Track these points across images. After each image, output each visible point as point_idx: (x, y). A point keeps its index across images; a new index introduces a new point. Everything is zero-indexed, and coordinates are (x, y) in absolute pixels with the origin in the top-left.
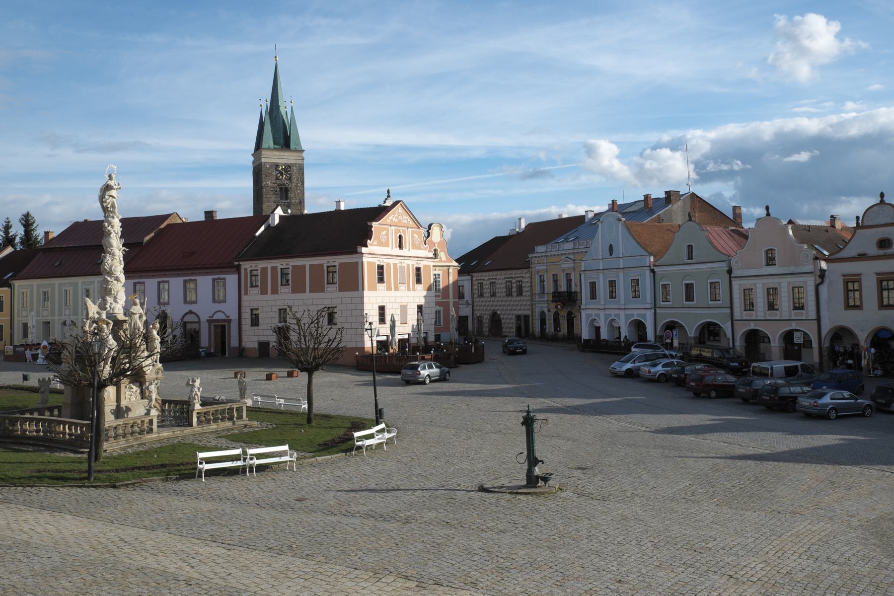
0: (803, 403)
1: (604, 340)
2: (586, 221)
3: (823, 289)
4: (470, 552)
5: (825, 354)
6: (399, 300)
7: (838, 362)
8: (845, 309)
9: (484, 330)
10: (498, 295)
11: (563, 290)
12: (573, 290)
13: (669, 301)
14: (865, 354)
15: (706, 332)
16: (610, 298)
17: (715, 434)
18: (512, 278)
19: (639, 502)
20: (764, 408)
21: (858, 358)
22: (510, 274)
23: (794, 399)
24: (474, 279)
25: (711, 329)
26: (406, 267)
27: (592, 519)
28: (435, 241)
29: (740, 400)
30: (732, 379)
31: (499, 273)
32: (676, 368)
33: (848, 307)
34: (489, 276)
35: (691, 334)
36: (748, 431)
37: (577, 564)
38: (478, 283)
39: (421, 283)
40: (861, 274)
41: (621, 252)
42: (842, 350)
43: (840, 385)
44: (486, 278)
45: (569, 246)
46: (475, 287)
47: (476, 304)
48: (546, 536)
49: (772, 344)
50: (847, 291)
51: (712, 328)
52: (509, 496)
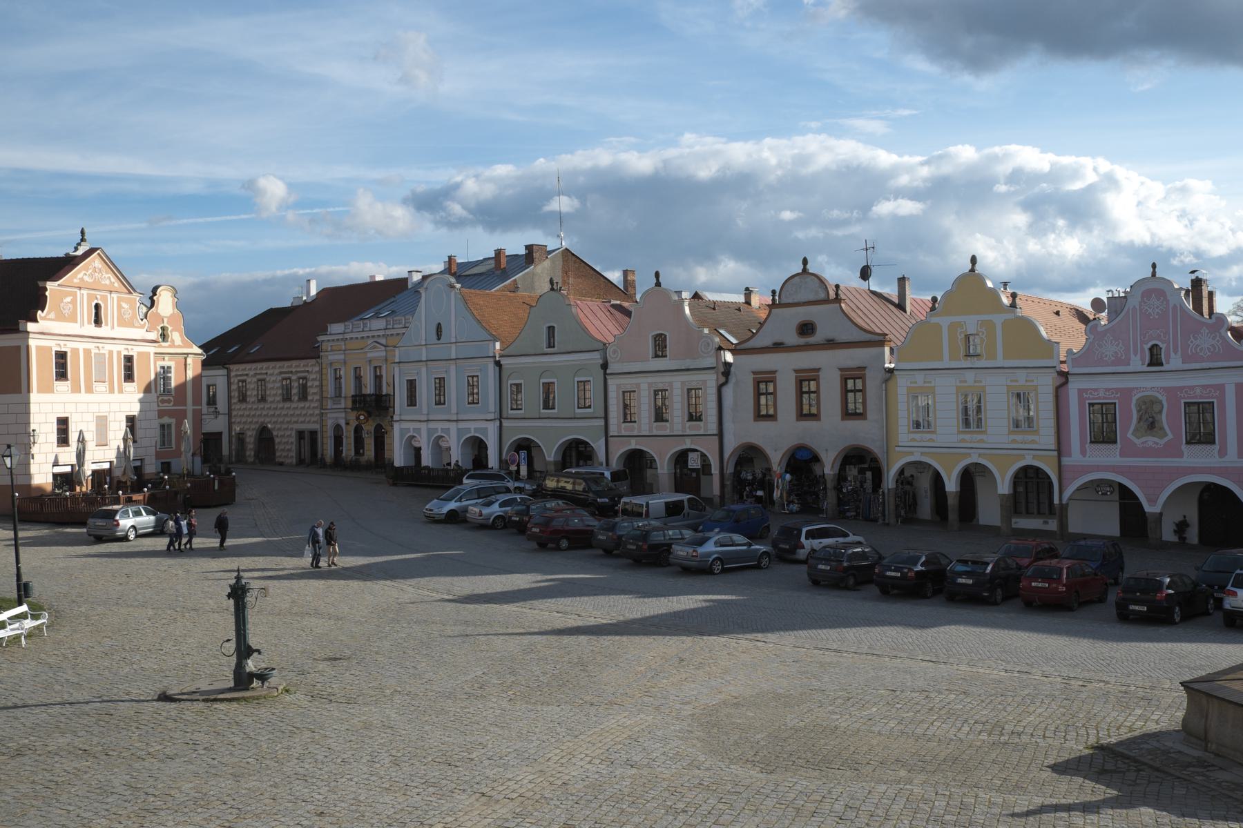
0: (679, 553)
1: (427, 468)
2: (409, 287)
3: (728, 392)
5: (728, 483)
6: (94, 408)
7: (745, 493)
8: (755, 420)
9: (248, 453)
10: (269, 399)
11: (369, 392)
12: (384, 392)
13: (521, 409)
14: (778, 482)
15: (574, 454)
16: (436, 404)
18: (291, 372)
20: (630, 561)
22: (288, 367)
24: (233, 374)
25: (581, 449)
26: (107, 356)
28: (162, 314)
29: (601, 552)
30: (593, 522)
31: (272, 364)
32: (520, 508)
33: (759, 416)
34: (255, 369)
35: (550, 456)
36: (595, 595)
38: (239, 381)
39: (133, 381)
40: (776, 371)
41: (453, 335)
42: (750, 478)
43: (736, 525)
44: (252, 373)
45: (379, 324)
46: (234, 387)
47: (234, 413)
49: (659, 471)
50: (758, 394)
52: (201, 705)
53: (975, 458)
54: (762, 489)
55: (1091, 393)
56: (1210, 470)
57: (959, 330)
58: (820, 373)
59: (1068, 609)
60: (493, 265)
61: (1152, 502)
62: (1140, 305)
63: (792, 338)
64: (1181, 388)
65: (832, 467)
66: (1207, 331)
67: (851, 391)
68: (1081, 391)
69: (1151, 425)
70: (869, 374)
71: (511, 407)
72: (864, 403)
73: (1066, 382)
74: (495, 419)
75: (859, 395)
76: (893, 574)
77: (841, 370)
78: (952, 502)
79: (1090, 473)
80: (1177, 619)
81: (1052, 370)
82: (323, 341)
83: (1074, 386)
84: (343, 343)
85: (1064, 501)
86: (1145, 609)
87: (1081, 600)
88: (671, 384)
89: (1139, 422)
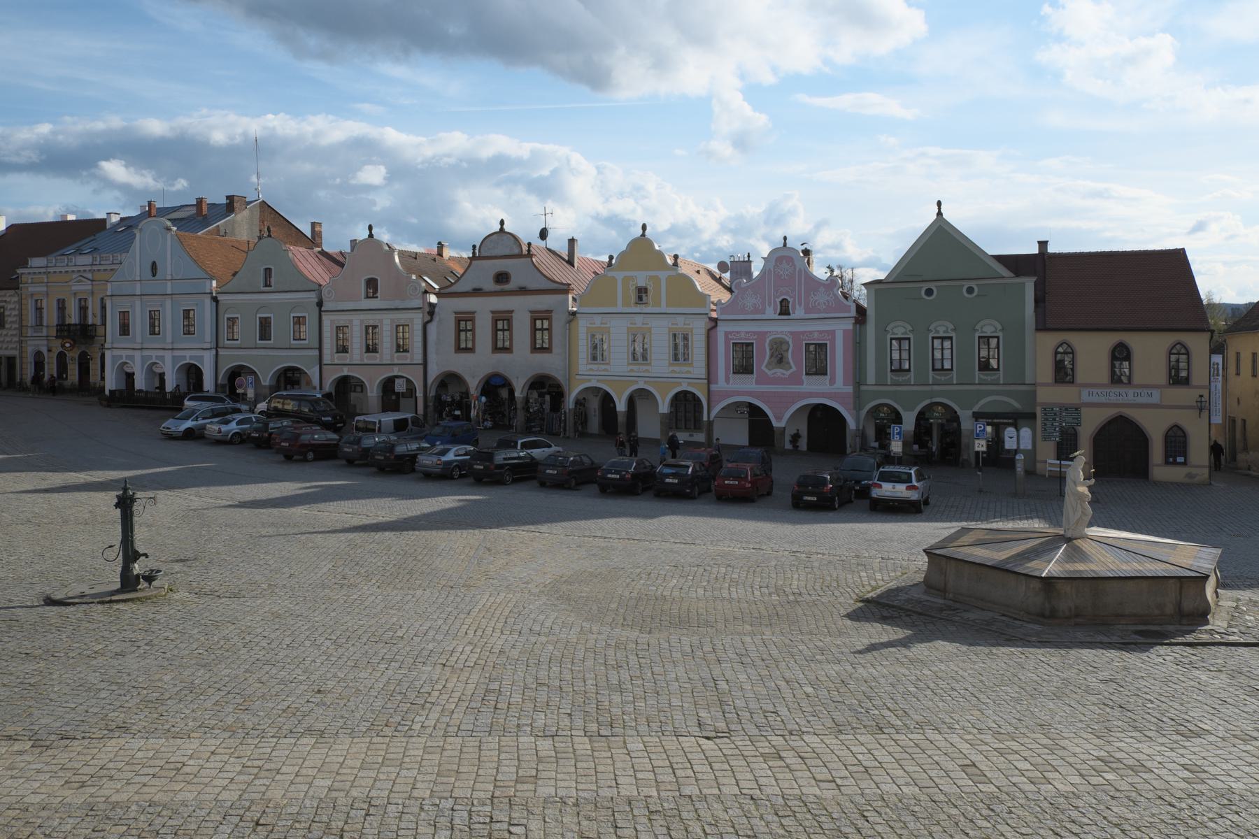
1: (140, 391)
2: (108, 227)
3: (433, 329)
4: (89, 688)
7: (444, 414)
8: (456, 352)
11: (73, 322)
15: (282, 379)
17: (331, 503)
20: (374, 469)
21: (467, 409)
23: (413, 458)
27: (236, 622)
29: (344, 462)
30: (333, 436)
33: (459, 349)
35: (265, 381)
36: (369, 498)
37: (251, 681)
42: (449, 400)
43: (456, 439)
45: (86, 260)
48: (187, 652)
49: (369, 394)
50: (459, 330)
51: (289, 374)
52: (100, 607)
53: (641, 385)
54: (460, 408)
56: (823, 395)
57: (631, 283)
59: (753, 501)
61: (779, 419)
62: (774, 268)
63: (490, 285)
64: (803, 333)
67: (539, 330)
68: (727, 334)
70: (554, 316)
72: (511, 340)
73: (716, 326)
75: (546, 333)
76: (613, 476)
77: (531, 312)
78: (621, 419)
80: (837, 506)
81: (705, 316)
82: (22, 274)
83: (722, 329)
84: (45, 276)
85: (711, 419)
86: (816, 499)
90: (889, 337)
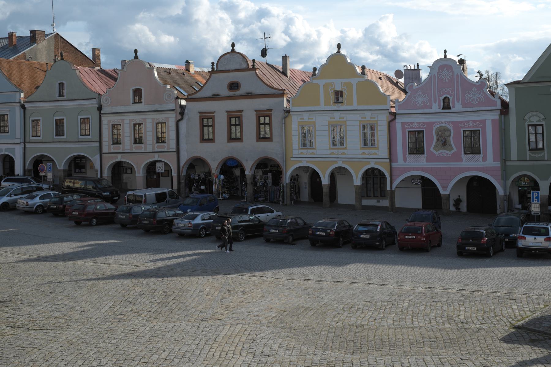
0: (179, 225)
3: (183, 125)
14: (215, 180)
15: (73, 165)
17: (110, 257)
19: (76, 326)
21: (209, 184)
23: (170, 222)
25: (77, 162)
29: (119, 226)
30: (109, 206)
32: (53, 200)
33: (203, 140)
35: (60, 166)
36: (138, 253)
42: (196, 178)
43: (202, 208)
49: (137, 175)
50: (202, 126)
51: (78, 161)
53: (340, 164)
54: (204, 184)
55: (409, 125)
56: (478, 169)
58: (243, 113)
59: (427, 251)
60: (8, 43)
61: (445, 188)
62: (438, 74)
63: (225, 92)
65: (251, 170)
66: (476, 89)
67: (263, 124)
68: (403, 124)
69: (444, 143)
70: (274, 114)
71: (32, 135)
72: (242, 132)
73: (395, 118)
74: (20, 143)
75: (267, 126)
76: (321, 233)
77: (256, 111)
78: (326, 190)
79: (409, 171)
80: (492, 254)
81: (387, 111)
83: (399, 121)
85: (393, 189)
86: (475, 249)
87: (432, 245)
88: (145, 120)
89: (437, 142)
90: (527, 124)
